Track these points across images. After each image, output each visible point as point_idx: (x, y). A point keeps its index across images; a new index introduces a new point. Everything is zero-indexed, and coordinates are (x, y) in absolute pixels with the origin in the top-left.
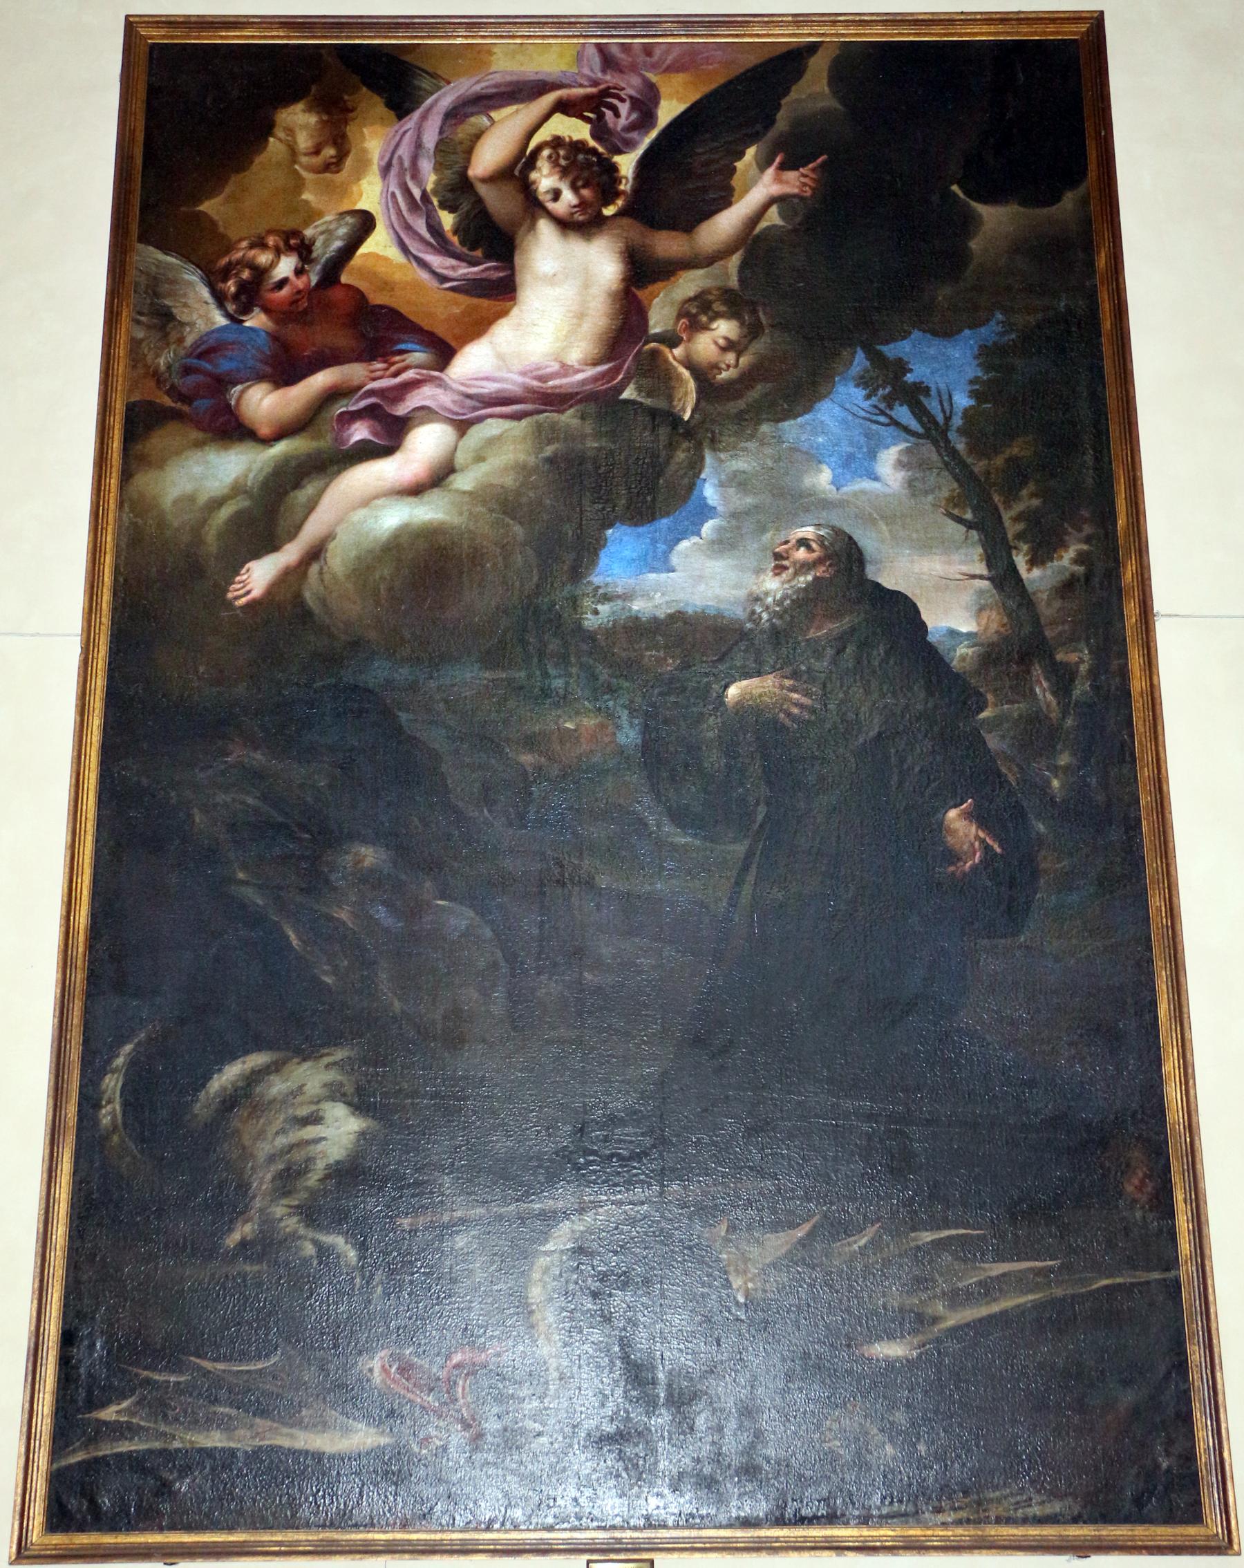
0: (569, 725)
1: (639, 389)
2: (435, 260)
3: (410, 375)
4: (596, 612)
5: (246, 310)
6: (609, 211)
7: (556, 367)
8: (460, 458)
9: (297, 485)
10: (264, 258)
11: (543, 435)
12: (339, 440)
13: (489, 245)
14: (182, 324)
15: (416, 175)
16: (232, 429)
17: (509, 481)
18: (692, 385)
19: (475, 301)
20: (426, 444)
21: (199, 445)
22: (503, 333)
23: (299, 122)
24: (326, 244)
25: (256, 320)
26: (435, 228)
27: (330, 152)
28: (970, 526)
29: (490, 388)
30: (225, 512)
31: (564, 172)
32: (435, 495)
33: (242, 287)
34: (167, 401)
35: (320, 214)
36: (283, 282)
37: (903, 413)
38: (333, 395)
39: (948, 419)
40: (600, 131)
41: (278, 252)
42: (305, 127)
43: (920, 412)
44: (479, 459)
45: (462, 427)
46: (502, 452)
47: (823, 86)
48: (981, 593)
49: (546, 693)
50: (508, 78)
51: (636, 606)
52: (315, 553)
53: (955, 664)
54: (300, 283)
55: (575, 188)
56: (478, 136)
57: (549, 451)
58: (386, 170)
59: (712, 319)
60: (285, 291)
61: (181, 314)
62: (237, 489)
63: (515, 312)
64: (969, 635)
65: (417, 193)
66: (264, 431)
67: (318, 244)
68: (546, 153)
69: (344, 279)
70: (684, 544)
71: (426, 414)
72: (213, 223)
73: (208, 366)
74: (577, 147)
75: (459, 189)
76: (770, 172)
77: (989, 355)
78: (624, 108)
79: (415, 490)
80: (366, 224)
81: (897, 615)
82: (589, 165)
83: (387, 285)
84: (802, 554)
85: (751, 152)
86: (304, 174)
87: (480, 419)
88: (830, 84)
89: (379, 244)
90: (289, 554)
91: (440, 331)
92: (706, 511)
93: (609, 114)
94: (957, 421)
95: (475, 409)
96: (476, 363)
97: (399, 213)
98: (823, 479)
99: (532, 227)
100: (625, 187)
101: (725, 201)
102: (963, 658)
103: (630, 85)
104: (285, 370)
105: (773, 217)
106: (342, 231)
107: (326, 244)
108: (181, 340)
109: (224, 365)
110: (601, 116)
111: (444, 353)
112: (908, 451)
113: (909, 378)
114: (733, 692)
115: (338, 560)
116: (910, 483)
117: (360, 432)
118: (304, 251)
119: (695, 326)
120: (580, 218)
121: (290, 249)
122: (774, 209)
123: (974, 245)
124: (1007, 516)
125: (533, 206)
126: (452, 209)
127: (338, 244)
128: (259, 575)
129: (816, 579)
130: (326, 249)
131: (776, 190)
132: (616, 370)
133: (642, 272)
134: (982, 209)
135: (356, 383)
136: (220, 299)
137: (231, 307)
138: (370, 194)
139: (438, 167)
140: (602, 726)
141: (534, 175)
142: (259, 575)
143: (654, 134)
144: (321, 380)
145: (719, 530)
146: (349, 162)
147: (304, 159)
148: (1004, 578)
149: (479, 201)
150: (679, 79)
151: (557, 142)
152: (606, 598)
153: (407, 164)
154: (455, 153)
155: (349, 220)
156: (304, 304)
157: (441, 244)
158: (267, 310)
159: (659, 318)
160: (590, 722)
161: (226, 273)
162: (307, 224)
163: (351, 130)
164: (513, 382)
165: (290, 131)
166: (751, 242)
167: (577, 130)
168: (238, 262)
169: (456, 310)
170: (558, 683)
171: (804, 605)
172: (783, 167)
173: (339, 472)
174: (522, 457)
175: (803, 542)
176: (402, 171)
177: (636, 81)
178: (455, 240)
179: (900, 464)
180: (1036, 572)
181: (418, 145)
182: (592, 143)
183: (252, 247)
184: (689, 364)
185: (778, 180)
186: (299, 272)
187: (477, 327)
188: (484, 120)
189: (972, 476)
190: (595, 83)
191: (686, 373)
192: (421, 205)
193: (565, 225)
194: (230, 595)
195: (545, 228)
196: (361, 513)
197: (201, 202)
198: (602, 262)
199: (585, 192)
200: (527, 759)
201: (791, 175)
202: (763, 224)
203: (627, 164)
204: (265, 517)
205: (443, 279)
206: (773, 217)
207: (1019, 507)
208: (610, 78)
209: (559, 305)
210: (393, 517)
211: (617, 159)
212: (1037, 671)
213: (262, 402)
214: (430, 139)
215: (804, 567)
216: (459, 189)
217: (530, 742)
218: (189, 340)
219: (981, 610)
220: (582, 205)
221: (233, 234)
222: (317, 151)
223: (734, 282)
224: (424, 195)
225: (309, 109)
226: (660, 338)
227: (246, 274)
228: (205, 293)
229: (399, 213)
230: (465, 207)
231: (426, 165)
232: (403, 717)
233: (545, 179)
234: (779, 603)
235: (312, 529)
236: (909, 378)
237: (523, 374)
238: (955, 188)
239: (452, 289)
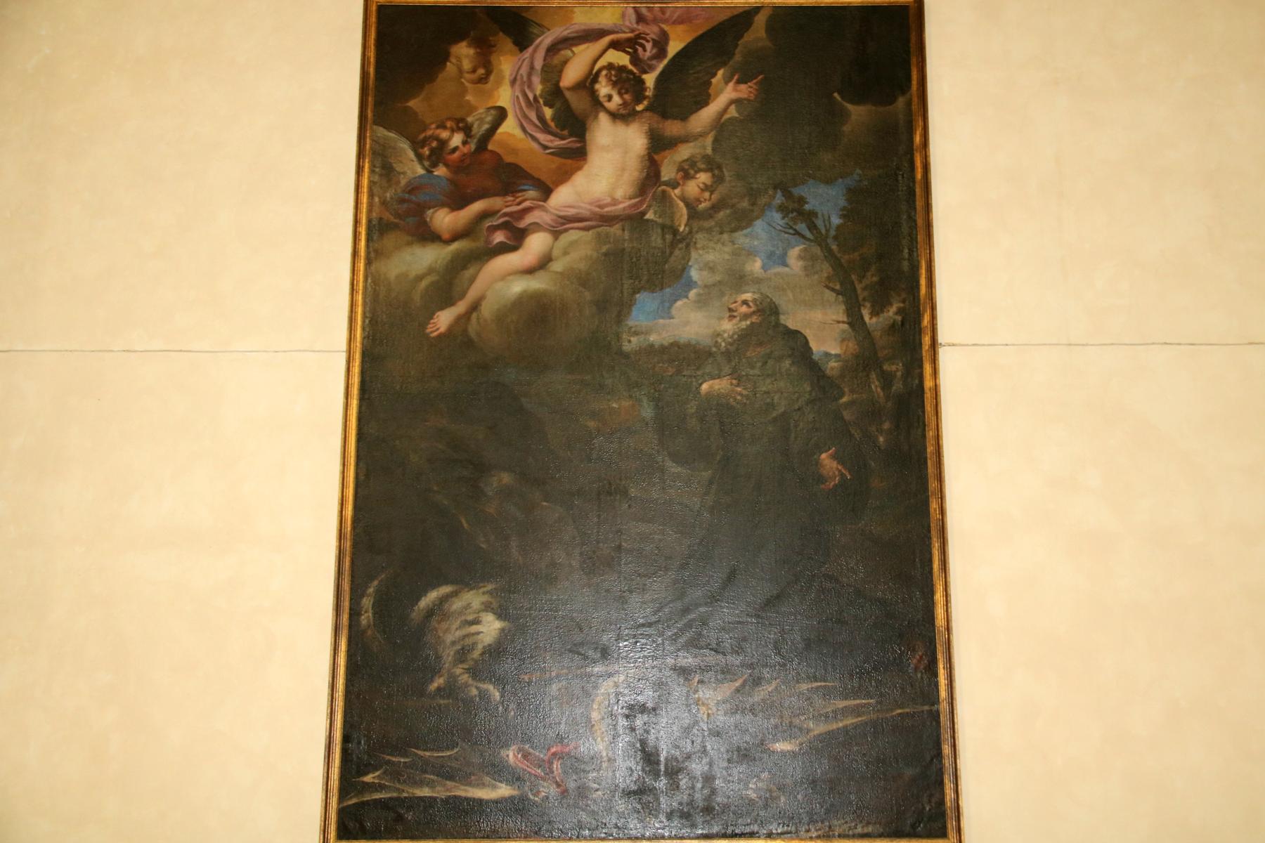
0: (614, 405)
1: (655, 213)
2: (542, 137)
3: (527, 204)
4: (630, 341)
5: (435, 165)
6: (639, 108)
7: (609, 200)
8: (555, 253)
9: (464, 267)
10: (444, 134)
11: (600, 239)
12: (488, 242)
13: (571, 125)
14: (399, 173)
15: (530, 86)
16: (428, 236)
17: (582, 266)
18: (685, 211)
19: (563, 160)
20: (537, 243)
21: (409, 244)
22: (579, 179)
23: (464, 52)
24: (480, 126)
25: (441, 171)
26: (541, 118)
27: (481, 71)
28: (838, 293)
29: (572, 212)
30: (424, 284)
31: (614, 84)
32: (541, 273)
33: (432, 151)
34: (392, 219)
35: (476, 109)
36: (456, 149)
37: (802, 227)
38: (484, 215)
39: (828, 231)
40: (635, 60)
41: (453, 131)
42: (467, 56)
43: (812, 227)
44: (566, 253)
45: (556, 234)
46: (578, 250)
47: (762, 33)
48: (844, 331)
49: (602, 386)
50: (583, 27)
51: (653, 338)
52: (475, 307)
53: (828, 372)
54: (465, 150)
55: (620, 94)
56: (565, 62)
57: (604, 249)
58: (513, 82)
59: (696, 172)
60: (457, 154)
61: (398, 167)
62: (431, 271)
63: (586, 167)
64: (837, 356)
65: (531, 97)
66: (446, 236)
67: (475, 126)
68: (604, 73)
69: (490, 147)
70: (679, 303)
71: (536, 227)
72: (416, 114)
73: (414, 198)
74: (622, 69)
75: (555, 94)
76: (731, 84)
77: (852, 193)
78: (649, 46)
79: (530, 271)
80: (502, 114)
81: (797, 343)
82: (628, 80)
83: (514, 151)
84: (744, 309)
85: (720, 73)
86: (467, 84)
87: (566, 230)
88: (766, 31)
89: (510, 127)
90: (461, 307)
91: (543, 177)
92: (690, 284)
93: (640, 49)
94: (833, 233)
95: (563, 224)
96: (564, 197)
97: (521, 108)
98: (756, 266)
99: (596, 117)
100: (649, 93)
101: (704, 102)
102: (832, 369)
103: (652, 31)
104: (458, 201)
105: (733, 112)
106: (489, 119)
107: (480, 126)
108: (399, 182)
109: (421, 197)
110: (636, 51)
111: (546, 191)
112: (805, 249)
113: (807, 207)
114: (705, 387)
115: (487, 310)
116: (806, 268)
117: (499, 237)
118: (467, 130)
119: (687, 176)
120: (623, 112)
121: (459, 129)
122: (733, 107)
123: (846, 128)
124: (859, 287)
125: (597, 104)
126: (551, 106)
127: (486, 126)
128: (444, 320)
129: (752, 323)
130: (479, 129)
131: (734, 95)
132: (641, 202)
133: (658, 144)
134: (849, 106)
135: (497, 208)
136: (420, 157)
137: (426, 163)
138: (505, 97)
139: (544, 81)
140: (633, 406)
141: (597, 86)
142: (444, 320)
143: (666, 62)
144: (477, 207)
145: (699, 295)
146: (492, 78)
147: (467, 76)
148: (855, 321)
149: (566, 102)
150: (680, 28)
151: (610, 66)
152: (636, 334)
153: (525, 79)
154: (552, 72)
155: (493, 112)
156: (468, 161)
157: (545, 128)
158: (446, 165)
159: (668, 172)
160: (626, 403)
161: (424, 143)
162: (469, 114)
163: (494, 58)
164: (585, 209)
165: (459, 59)
166: (721, 127)
167: (622, 59)
168: (430, 137)
169: (553, 166)
170: (609, 382)
171: (744, 338)
172: (738, 82)
173: (488, 261)
174: (589, 253)
175: (745, 302)
176: (523, 83)
177: (655, 29)
178: (552, 124)
179: (800, 257)
180: (874, 320)
181: (532, 67)
182: (631, 67)
183: (438, 127)
184: (683, 199)
185: (735, 90)
186: (465, 143)
187: (564, 176)
188: (569, 53)
189: (841, 265)
190: (632, 31)
191: (681, 204)
192: (533, 104)
193: (614, 116)
194: (428, 331)
195: (603, 118)
196: (500, 285)
197: (407, 101)
198: (635, 138)
199: (627, 97)
200: (592, 424)
201: (743, 87)
202: (727, 116)
203: (650, 79)
204: (446, 287)
205: (545, 147)
206: (733, 112)
207: (866, 282)
208: (641, 28)
209: (611, 162)
210: (518, 287)
211: (644, 76)
212: (873, 376)
213: (444, 219)
214: (539, 64)
215: (745, 317)
216: (555, 94)
217: (594, 415)
218: (403, 182)
219: (843, 340)
220: (625, 104)
221: (428, 122)
222: (474, 71)
223: (709, 151)
224: (535, 98)
225: (469, 46)
226: (667, 184)
227: (434, 144)
228: (411, 154)
229: (521, 108)
230: (558, 105)
231: (536, 80)
232: (523, 399)
233: (603, 89)
234: (732, 337)
235: (472, 294)
236: (807, 207)
237: (591, 204)
238: (836, 95)
239: (551, 154)
